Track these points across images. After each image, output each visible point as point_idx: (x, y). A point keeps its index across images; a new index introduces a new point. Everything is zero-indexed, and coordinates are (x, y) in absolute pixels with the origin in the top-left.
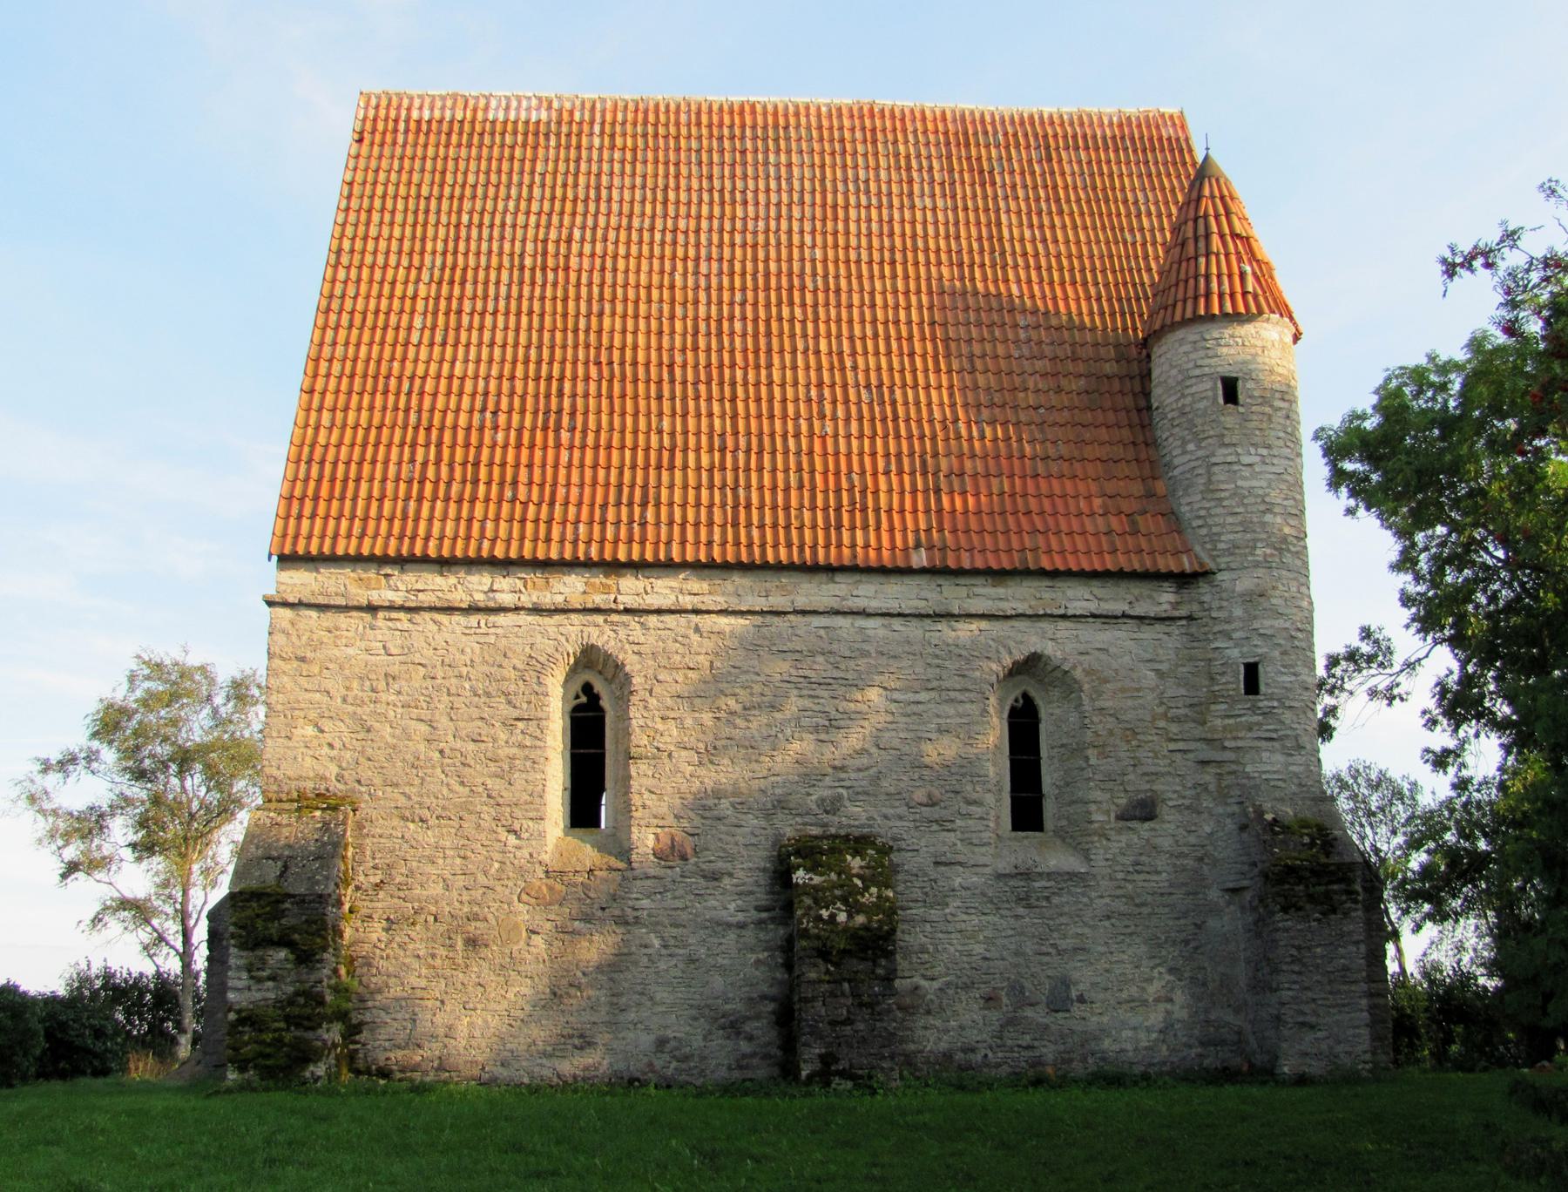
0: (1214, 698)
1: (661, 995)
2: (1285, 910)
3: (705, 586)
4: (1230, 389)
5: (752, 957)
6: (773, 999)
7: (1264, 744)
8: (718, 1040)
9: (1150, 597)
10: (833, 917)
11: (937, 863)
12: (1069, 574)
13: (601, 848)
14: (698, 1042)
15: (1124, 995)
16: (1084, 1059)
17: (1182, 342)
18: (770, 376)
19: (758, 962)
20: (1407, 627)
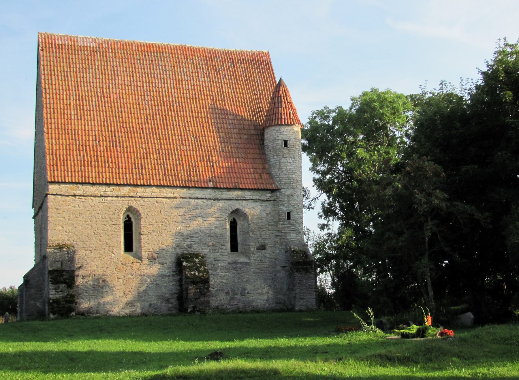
0: (280, 220)
1: (150, 293)
2: (297, 272)
4: (286, 143)
5: (172, 284)
6: (177, 294)
8: (164, 304)
10: (195, 274)
11: (215, 260)
12: (246, 189)
13: (134, 257)
14: (159, 304)
15: (258, 292)
16: (249, 307)
17: (274, 130)
18: (168, 132)
19: (173, 285)
20: (313, 186)
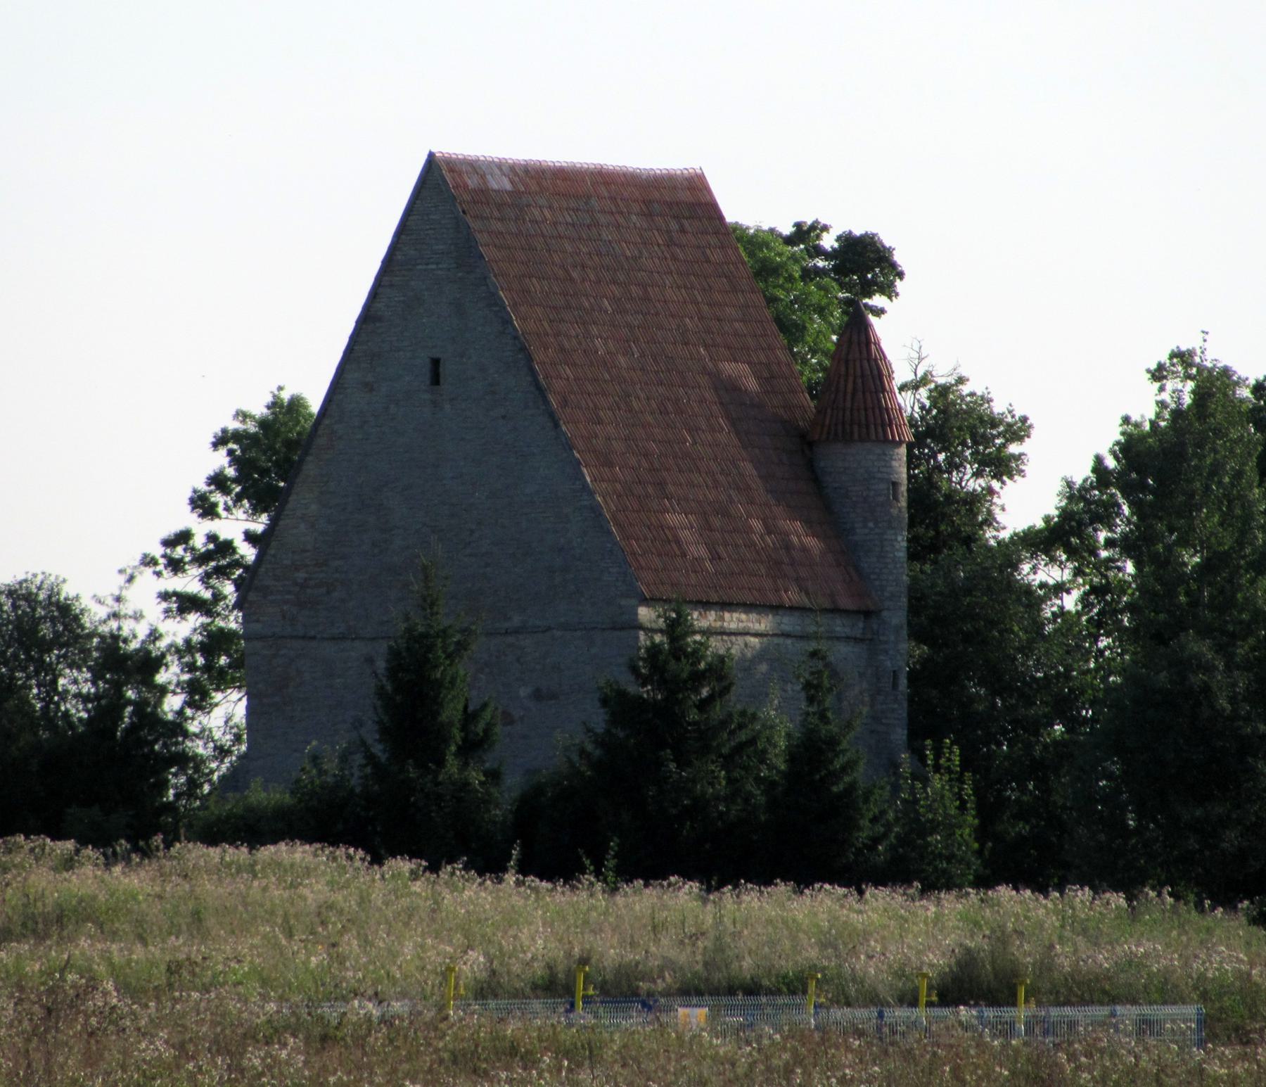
3: (743, 616)
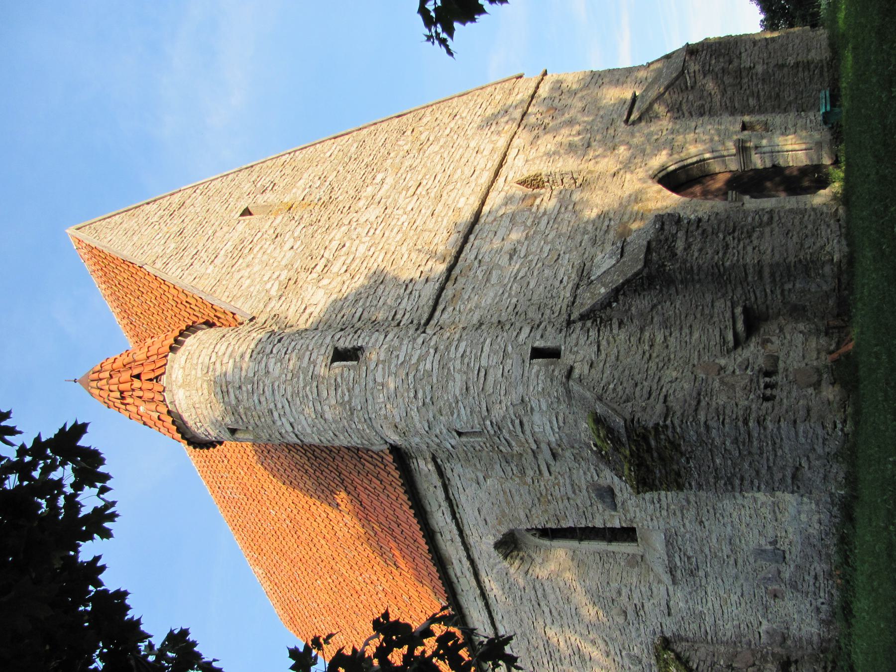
7: (527, 427)
9: (426, 476)
11: (669, 614)
